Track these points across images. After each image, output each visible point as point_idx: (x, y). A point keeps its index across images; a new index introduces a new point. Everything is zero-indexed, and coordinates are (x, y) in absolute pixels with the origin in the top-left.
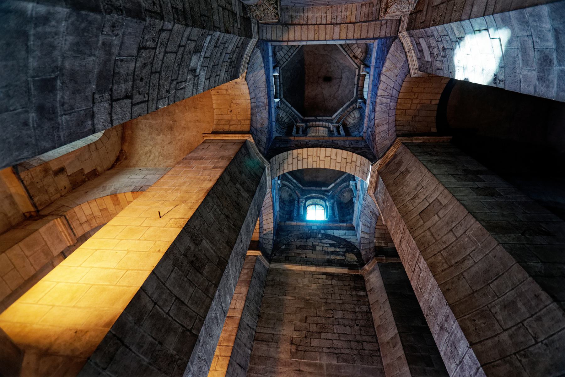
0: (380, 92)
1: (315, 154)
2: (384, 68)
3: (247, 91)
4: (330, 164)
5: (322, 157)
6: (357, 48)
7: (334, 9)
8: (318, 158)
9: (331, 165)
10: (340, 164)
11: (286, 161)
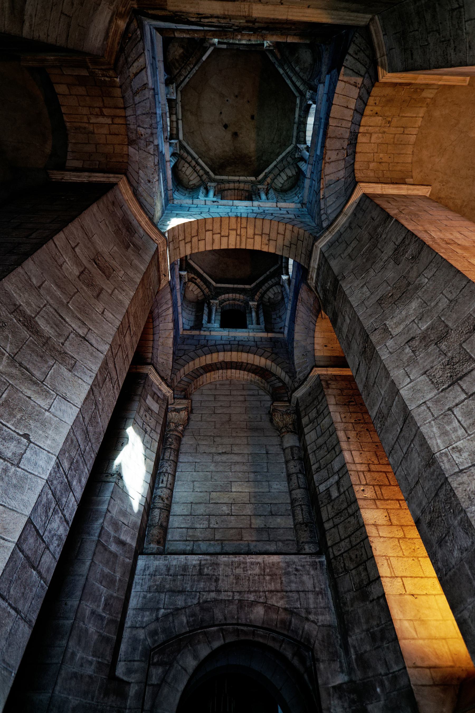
0: (171, 310)
1: (244, 239)
2: (172, 336)
3: (317, 335)
4: (221, 225)
5: (233, 233)
6: (194, 290)
7: (225, 378)
8: (239, 233)
9: (219, 224)
10: (207, 228)
11: (287, 243)
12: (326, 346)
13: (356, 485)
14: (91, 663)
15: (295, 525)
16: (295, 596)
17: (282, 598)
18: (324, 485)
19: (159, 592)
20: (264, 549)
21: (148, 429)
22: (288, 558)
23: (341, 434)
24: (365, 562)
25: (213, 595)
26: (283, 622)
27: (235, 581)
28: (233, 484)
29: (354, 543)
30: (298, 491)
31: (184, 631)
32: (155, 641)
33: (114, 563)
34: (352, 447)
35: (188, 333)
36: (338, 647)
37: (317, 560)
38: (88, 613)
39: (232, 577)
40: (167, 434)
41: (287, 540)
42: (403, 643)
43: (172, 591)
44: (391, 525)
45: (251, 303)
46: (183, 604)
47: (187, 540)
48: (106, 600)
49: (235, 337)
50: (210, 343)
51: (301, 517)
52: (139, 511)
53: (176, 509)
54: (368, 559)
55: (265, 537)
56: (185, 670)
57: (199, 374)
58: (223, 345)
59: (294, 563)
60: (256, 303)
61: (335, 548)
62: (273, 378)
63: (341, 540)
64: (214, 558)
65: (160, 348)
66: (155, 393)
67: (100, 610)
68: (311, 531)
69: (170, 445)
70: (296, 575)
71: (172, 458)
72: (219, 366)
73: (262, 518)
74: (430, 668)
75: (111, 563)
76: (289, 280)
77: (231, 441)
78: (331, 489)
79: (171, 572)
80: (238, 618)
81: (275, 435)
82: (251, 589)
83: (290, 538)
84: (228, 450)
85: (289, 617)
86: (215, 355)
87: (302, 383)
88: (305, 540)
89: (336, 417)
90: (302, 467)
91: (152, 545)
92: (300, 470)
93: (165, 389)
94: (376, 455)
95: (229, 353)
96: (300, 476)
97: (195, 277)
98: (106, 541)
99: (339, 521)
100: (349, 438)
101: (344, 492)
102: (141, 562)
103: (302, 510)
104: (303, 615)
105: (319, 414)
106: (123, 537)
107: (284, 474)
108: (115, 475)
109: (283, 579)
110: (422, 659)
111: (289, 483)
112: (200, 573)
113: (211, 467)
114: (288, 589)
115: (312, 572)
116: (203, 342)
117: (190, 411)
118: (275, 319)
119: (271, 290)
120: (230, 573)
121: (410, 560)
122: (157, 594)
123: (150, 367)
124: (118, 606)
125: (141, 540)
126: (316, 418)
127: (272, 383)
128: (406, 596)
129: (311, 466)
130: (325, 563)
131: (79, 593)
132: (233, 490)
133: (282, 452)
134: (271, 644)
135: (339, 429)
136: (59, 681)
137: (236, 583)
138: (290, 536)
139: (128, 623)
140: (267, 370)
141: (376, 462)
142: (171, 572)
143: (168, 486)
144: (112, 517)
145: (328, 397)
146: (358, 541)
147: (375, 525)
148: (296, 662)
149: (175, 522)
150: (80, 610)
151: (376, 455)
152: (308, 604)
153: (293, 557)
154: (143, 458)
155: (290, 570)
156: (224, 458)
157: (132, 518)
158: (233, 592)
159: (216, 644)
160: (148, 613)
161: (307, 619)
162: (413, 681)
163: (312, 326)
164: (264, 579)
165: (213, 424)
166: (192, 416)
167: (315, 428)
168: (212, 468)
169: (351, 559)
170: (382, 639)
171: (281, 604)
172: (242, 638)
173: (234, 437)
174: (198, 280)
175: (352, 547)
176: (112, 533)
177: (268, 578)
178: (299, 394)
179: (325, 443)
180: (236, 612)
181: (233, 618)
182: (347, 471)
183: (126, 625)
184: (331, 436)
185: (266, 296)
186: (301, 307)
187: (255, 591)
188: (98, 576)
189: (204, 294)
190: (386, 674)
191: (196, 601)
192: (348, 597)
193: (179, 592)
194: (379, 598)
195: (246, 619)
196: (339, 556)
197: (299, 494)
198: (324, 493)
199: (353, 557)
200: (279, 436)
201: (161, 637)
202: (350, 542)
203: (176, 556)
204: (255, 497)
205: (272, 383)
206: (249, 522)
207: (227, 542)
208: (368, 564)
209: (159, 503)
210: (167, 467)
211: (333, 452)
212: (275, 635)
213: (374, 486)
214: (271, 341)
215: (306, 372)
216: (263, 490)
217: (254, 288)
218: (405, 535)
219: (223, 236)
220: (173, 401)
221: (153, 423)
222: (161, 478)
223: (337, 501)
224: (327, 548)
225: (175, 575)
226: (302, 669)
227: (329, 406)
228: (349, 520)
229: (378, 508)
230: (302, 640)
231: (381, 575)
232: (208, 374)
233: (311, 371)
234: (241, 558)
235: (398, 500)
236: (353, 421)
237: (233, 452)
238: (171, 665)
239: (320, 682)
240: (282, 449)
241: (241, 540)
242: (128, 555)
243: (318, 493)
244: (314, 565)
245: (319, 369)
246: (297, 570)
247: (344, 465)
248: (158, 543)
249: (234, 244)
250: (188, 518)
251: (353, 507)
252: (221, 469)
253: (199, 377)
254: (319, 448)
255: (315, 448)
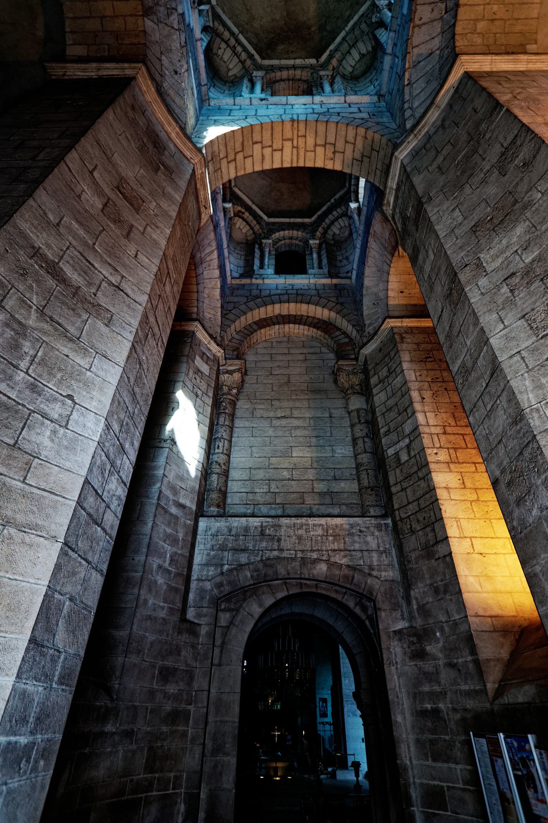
0: (215, 254)
2: (219, 286)
3: (392, 278)
5: (288, 144)
6: (241, 227)
7: (282, 335)
10: (255, 140)
12: (402, 292)
13: (429, 448)
14: (163, 608)
15: (360, 490)
16: (359, 554)
17: (345, 556)
18: (393, 448)
19: (222, 550)
20: (326, 512)
21: (200, 393)
22: (352, 520)
23: (415, 395)
24: (433, 524)
25: (276, 553)
26: (346, 577)
27: (297, 541)
28: (294, 449)
29: (422, 506)
30: (364, 455)
31: (248, 584)
32: (222, 591)
33: (176, 524)
34: (426, 408)
35: (238, 281)
36: (400, 599)
37: (382, 522)
38: (155, 566)
39: (294, 537)
40: (220, 398)
41: (351, 504)
42: (465, 596)
43: (236, 550)
44: (465, 488)
45: (311, 242)
46: (247, 561)
47: (247, 504)
48: (171, 557)
49: (293, 285)
50: (264, 293)
51: (367, 481)
52: (196, 476)
53: (234, 474)
54: (437, 521)
55: (328, 500)
56: (252, 616)
57: (252, 330)
58: (279, 295)
59: (358, 525)
60: (318, 242)
61: (401, 510)
62: (338, 333)
63: (409, 503)
64: (275, 520)
65: (206, 301)
66: (204, 353)
67: (166, 565)
68: (377, 495)
69: (224, 409)
70: (359, 535)
71: (226, 423)
72: (274, 320)
73: (325, 482)
74: (491, 617)
75: (172, 524)
76: (359, 209)
77: (291, 404)
78: (400, 453)
79: (233, 533)
80: (301, 573)
81: (340, 396)
82: (314, 548)
83: (355, 502)
84: (288, 413)
85: (351, 573)
86: (270, 308)
87: (372, 337)
88: (370, 503)
89: (410, 375)
90: (369, 431)
91: (212, 509)
92: (367, 434)
93: (215, 348)
94: (454, 416)
95: (286, 305)
96: (367, 440)
97: (243, 210)
98: (166, 504)
99: (407, 485)
100: (424, 398)
101: (415, 456)
102: (203, 523)
103: (368, 474)
104: (366, 571)
105: (390, 372)
106: (182, 501)
107: (349, 438)
108: (169, 441)
109: (347, 539)
110: (485, 609)
111: (354, 447)
112: (262, 533)
113: (270, 432)
114: (352, 548)
115: (377, 533)
116: (255, 292)
117: (244, 373)
118: (341, 261)
119: (336, 223)
120: (292, 534)
121: (482, 522)
122: (220, 552)
123: (196, 323)
124: (184, 562)
125: (200, 503)
126: (387, 377)
127: (336, 339)
128: (473, 555)
129: (379, 430)
130: (391, 525)
131: (145, 550)
132: (294, 455)
133: (347, 415)
134: (334, 595)
135: (413, 388)
136: (135, 621)
137: (299, 543)
138: (355, 500)
139: (194, 576)
140: (331, 324)
141: (453, 423)
142: (233, 533)
143: (225, 452)
144: (169, 482)
145: (401, 353)
146: (428, 504)
147: (447, 488)
148: (358, 610)
149: (233, 486)
150: (147, 565)
151: (454, 416)
152: (372, 561)
153: (358, 519)
154: (196, 423)
155: (354, 531)
156: (284, 422)
157: (189, 482)
158: (296, 551)
159: (280, 595)
160: (212, 568)
161: (370, 575)
162: (473, 627)
163: (386, 268)
164: (327, 539)
165: (270, 386)
166: (247, 378)
167: (385, 389)
168: (271, 432)
169: (418, 521)
170: (445, 592)
171: (344, 561)
172: (305, 590)
173: (294, 400)
174: (247, 214)
175: (420, 510)
176: (171, 497)
177: (331, 538)
178: (367, 350)
179: (396, 404)
180: (299, 568)
181: (296, 573)
182: (420, 434)
183: (192, 578)
184: (403, 396)
185: (330, 232)
186: (374, 243)
187: (318, 550)
188: (161, 535)
189: (254, 233)
190: (447, 622)
191: (259, 559)
192: (413, 555)
193: (242, 550)
194: (445, 556)
195: (309, 574)
196: (406, 518)
197: (364, 458)
198: (393, 457)
199: (421, 519)
200: (344, 398)
201: (227, 589)
202: (419, 505)
203: (237, 519)
204: (317, 462)
205: (336, 339)
206: (311, 487)
207: (288, 506)
208: (436, 525)
209: (216, 469)
210: (222, 432)
211: (405, 413)
212: (337, 588)
213: (448, 449)
214: (336, 289)
215: (376, 325)
216: (326, 455)
217: (315, 222)
218: (478, 498)
219: (276, 150)
220: (224, 361)
221: (204, 386)
222: (217, 443)
223: (406, 464)
224: (394, 511)
225: (237, 535)
226: (363, 617)
227: (403, 363)
228: (419, 483)
229: (451, 472)
230: (365, 593)
231: (449, 535)
232: (263, 331)
233: (383, 323)
234: (303, 520)
235: (475, 463)
236: (430, 380)
237: (293, 416)
238: (237, 610)
239: (381, 627)
240: (348, 412)
241: (303, 504)
242: (189, 517)
243: (386, 457)
244: (379, 527)
245: (393, 320)
246: (361, 531)
247: (416, 428)
248: (218, 506)
249: (289, 160)
250: (247, 482)
251: (424, 470)
252: (280, 433)
253: (252, 333)
254: (390, 410)
255: (384, 410)
